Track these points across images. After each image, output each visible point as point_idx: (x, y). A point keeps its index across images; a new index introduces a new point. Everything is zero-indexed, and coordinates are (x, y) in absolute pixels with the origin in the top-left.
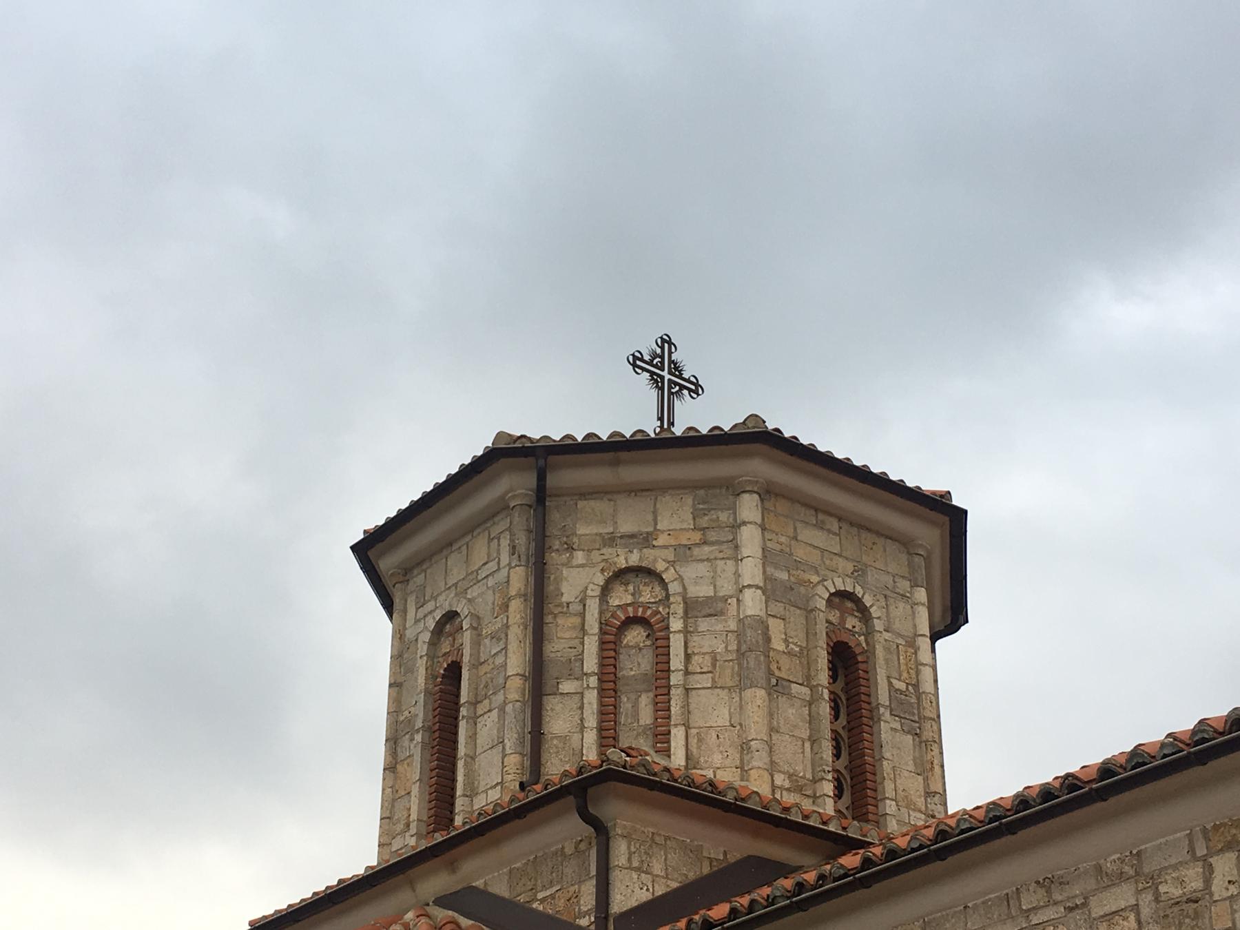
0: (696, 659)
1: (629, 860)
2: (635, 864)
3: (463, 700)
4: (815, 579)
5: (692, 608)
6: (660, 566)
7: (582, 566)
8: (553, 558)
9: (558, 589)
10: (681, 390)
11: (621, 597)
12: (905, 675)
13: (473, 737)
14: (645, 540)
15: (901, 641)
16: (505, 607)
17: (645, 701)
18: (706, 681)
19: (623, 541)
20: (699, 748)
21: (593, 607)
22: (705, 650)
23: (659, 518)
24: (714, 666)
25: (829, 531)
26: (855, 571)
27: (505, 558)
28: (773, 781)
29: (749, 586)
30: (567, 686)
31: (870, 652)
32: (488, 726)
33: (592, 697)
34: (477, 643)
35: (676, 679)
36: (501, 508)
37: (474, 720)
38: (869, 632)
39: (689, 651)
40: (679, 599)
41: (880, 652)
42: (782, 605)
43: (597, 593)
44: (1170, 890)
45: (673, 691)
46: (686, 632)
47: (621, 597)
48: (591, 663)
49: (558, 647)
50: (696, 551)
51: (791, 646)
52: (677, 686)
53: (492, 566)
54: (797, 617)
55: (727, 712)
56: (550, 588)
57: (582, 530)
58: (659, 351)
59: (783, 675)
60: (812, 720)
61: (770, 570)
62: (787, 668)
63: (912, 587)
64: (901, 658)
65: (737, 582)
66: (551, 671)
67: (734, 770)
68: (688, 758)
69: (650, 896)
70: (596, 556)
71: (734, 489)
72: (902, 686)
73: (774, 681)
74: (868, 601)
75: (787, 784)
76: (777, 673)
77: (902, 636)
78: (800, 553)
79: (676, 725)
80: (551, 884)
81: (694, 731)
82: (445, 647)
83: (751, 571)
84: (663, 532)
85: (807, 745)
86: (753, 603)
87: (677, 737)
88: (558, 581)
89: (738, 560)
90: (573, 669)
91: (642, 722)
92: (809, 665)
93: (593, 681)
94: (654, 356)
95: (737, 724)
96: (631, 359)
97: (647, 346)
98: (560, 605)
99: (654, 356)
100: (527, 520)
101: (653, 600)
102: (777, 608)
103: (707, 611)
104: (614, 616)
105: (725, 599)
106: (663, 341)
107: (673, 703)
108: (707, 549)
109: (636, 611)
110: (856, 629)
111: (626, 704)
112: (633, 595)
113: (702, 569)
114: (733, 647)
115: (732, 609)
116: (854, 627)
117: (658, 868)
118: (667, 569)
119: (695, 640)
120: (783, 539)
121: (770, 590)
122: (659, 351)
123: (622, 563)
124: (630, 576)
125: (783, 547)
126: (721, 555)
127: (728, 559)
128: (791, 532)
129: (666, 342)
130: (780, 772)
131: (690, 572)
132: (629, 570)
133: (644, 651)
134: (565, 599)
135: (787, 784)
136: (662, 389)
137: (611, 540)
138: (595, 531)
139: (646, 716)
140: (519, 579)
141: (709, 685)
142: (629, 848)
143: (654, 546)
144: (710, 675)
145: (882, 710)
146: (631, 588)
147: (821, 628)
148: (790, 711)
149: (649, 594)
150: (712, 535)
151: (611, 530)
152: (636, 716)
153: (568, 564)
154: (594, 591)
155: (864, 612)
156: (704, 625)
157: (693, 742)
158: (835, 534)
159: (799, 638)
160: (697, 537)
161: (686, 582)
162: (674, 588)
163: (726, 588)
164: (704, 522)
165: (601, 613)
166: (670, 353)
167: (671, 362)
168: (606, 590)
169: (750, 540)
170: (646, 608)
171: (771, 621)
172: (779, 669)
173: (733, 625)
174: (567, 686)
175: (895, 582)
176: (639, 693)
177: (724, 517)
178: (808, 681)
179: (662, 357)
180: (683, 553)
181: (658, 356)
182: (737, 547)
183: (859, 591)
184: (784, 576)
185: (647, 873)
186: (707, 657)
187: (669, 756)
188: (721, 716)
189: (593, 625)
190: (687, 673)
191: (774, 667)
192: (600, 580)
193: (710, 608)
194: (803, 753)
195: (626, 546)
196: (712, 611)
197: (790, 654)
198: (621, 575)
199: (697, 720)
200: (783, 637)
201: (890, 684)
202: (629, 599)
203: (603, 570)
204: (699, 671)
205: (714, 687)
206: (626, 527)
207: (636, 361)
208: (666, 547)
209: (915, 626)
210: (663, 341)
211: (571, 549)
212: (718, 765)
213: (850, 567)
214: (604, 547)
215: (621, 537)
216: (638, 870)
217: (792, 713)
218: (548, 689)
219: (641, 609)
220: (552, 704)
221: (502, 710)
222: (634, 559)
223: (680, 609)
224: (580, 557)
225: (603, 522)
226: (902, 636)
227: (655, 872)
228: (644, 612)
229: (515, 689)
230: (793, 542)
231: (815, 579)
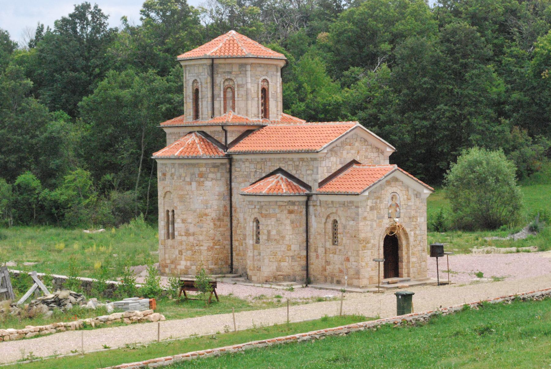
5: (238, 86)
6: (233, 78)
8: (215, 76)
11: (227, 83)
13: (202, 104)
14: (230, 73)
16: (207, 83)
17: (231, 101)
18: (241, 99)
27: (206, 74)
30: (218, 99)
31: (268, 88)
32: (205, 103)
33: (222, 102)
34: (202, 88)
35: (236, 99)
36: (206, 64)
37: (202, 101)
38: (268, 84)
44: (296, 164)
46: (238, 90)
47: (227, 83)
48: (222, 96)
49: (216, 92)
56: (214, 81)
60: (258, 104)
66: (215, 97)
71: (246, 64)
82: (195, 84)
90: (219, 96)
92: (258, 94)
102: (253, 85)
108: (241, 75)
115: (245, 87)
123: (227, 78)
137: (224, 73)
139: (231, 104)
140: (209, 80)
149: (231, 83)
150: (242, 72)
154: (222, 83)
155: (268, 82)
156: (241, 89)
159: (256, 89)
160: (239, 73)
162: (236, 83)
163: (244, 83)
164: (241, 70)
168: (224, 82)
169: (249, 73)
173: (245, 89)
174: (218, 99)
177: (244, 69)
180: (237, 75)
189: (222, 89)
192: (223, 80)
198: (226, 80)
206: (227, 70)
217: (255, 103)
220: (215, 102)
221: (207, 102)
222: (229, 77)
223: (236, 86)
224: (219, 75)
229: (210, 99)
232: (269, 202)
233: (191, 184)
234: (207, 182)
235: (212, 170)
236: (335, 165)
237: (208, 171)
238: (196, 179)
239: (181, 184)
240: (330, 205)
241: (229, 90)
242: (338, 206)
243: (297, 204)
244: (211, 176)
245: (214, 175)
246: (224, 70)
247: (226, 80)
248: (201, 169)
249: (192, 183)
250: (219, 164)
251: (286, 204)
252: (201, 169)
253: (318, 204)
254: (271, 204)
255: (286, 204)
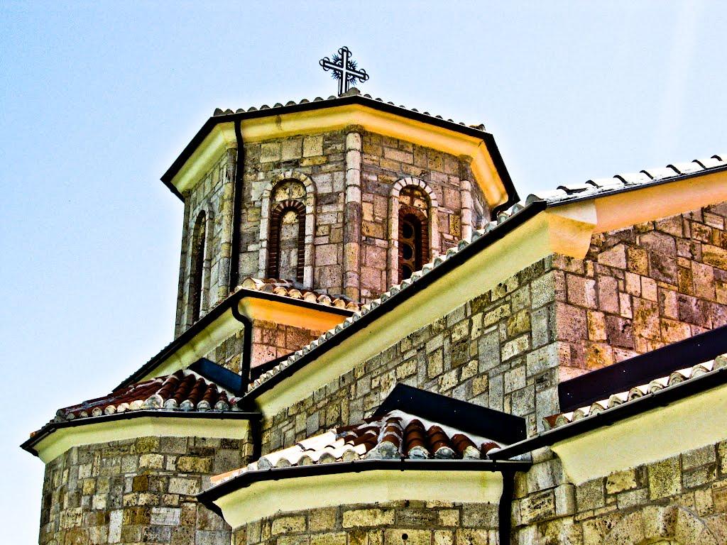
0: (321, 229)
1: (262, 339)
2: (266, 341)
3: (204, 259)
4: (394, 179)
5: (319, 200)
6: (303, 177)
7: (262, 180)
8: (248, 177)
9: (249, 194)
10: (353, 78)
12: (452, 231)
13: (208, 278)
15: (451, 212)
17: (294, 253)
18: (325, 240)
19: (284, 165)
20: (319, 277)
21: (266, 203)
22: (325, 223)
23: (305, 150)
24: (330, 231)
25: (406, 152)
26: (422, 173)
28: (360, 293)
29: (351, 185)
30: (252, 248)
31: (428, 221)
32: (215, 270)
33: (263, 253)
35: (308, 240)
37: (210, 268)
38: (428, 209)
39: (317, 224)
40: (312, 195)
41: (434, 219)
42: (372, 195)
43: (268, 195)
45: (306, 247)
46: (316, 214)
47: (282, 196)
48: (264, 234)
49: (246, 227)
50: (323, 168)
51: (377, 218)
52: (308, 244)
53: (220, 183)
54: (381, 201)
55: (336, 257)
57: (264, 160)
58: (340, 57)
59: (371, 234)
61: (365, 175)
62: (373, 230)
63: (460, 181)
64: (451, 221)
65: (344, 184)
67: (338, 288)
68: (314, 282)
69: (274, 358)
70: (270, 175)
72: (450, 237)
73: (364, 238)
74: (428, 190)
75: (369, 295)
76: (366, 233)
77: (450, 208)
78: (386, 165)
79: (307, 266)
80: (231, 354)
81: (317, 269)
83: (354, 177)
84: (305, 158)
85: (384, 273)
86: (354, 195)
87: (308, 271)
88: (250, 189)
89: (345, 171)
90: (254, 238)
91: (292, 265)
93: (264, 244)
94: (337, 59)
95: (341, 263)
96: (322, 62)
97: (332, 53)
98: (250, 203)
99: (337, 59)
100: (234, 157)
101: (299, 197)
103: (327, 201)
104: (279, 206)
105: (338, 194)
106: (343, 50)
107: (306, 253)
108: (329, 166)
109: (290, 203)
110: (421, 207)
111: (284, 256)
112: (289, 194)
113: (326, 177)
114: (341, 220)
115: (341, 200)
116: (420, 205)
117: (280, 343)
118: (306, 179)
119: (321, 217)
120: (374, 158)
121: (364, 187)
122: (340, 57)
123: (282, 177)
124: (288, 184)
125: (375, 162)
126: (337, 169)
127: (341, 171)
128: (380, 153)
129: (345, 51)
130: (365, 288)
131: (319, 179)
132: (286, 181)
133: (295, 226)
134: (253, 199)
135: (369, 295)
136: (342, 78)
137: (278, 165)
138: (270, 160)
139: (294, 262)
141: (327, 242)
142: (262, 333)
143: (301, 167)
144: (328, 237)
145: (433, 251)
146: (288, 191)
147: (396, 208)
148: (373, 254)
150: (332, 158)
151: (278, 159)
152: (289, 262)
153: (255, 180)
154: (266, 194)
156: (325, 209)
157: (317, 274)
158: (410, 153)
160: (324, 159)
161: (318, 185)
163: (339, 187)
165: (271, 205)
166: (347, 57)
167: (347, 62)
168: (273, 194)
170: (295, 201)
171: (364, 205)
172: (368, 231)
173: (341, 208)
175: (449, 178)
176: (290, 249)
177: (339, 147)
178: (387, 237)
179: (342, 60)
181: (340, 60)
182: (346, 164)
183: (422, 185)
184: (374, 178)
185: (273, 346)
186: (327, 227)
187: (303, 282)
188: (332, 260)
189: (265, 213)
190: (315, 236)
191: (364, 230)
192: (270, 187)
193: (331, 199)
194: (381, 277)
195: (286, 167)
196: (330, 201)
197: (375, 222)
198: (281, 184)
199: (319, 262)
200: (372, 213)
201: (442, 236)
202: (286, 197)
203: (272, 182)
204: (322, 234)
205: (330, 243)
206: (287, 156)
207: (325, 64)
208: (307, 167)
209: (461, 203)
210: (343, 50)
211: (256, 171)
212: (330, 286)
213: (418, 171)
214: (275, 168)
215: (284, 163)
216: (267, 344)
218: (242, 250)
219: (292, 203)
220: (244, 258)
222: (289, 175)
223: (311, 200)
224: (261, 175)
225: (274, 155)
226: (450, 208)
227: (279, 345)
228: (294, 204)
230: (381, 160)
231: (394, 179)
232: (307, 515)
233: (108, 519)
234: (163, 510)
235: (188, 464)
236: (653, 319)
237: (170, 466)
238: (127, 498)
239: (79, 520)
240: (633, 498)
241: (290, 217)
242: (675, 488)
243: (450, 519)
244: (180, 486)
245: (193, 482)
246: (276, 159)
247: (281, 184)
248: (144, 461)
249: (113, 515)
250: (217, 444)
251: (388, 518)
252: (144, 461)
253: (563, 506)
254: (313, 526)
255: (388, 518)
